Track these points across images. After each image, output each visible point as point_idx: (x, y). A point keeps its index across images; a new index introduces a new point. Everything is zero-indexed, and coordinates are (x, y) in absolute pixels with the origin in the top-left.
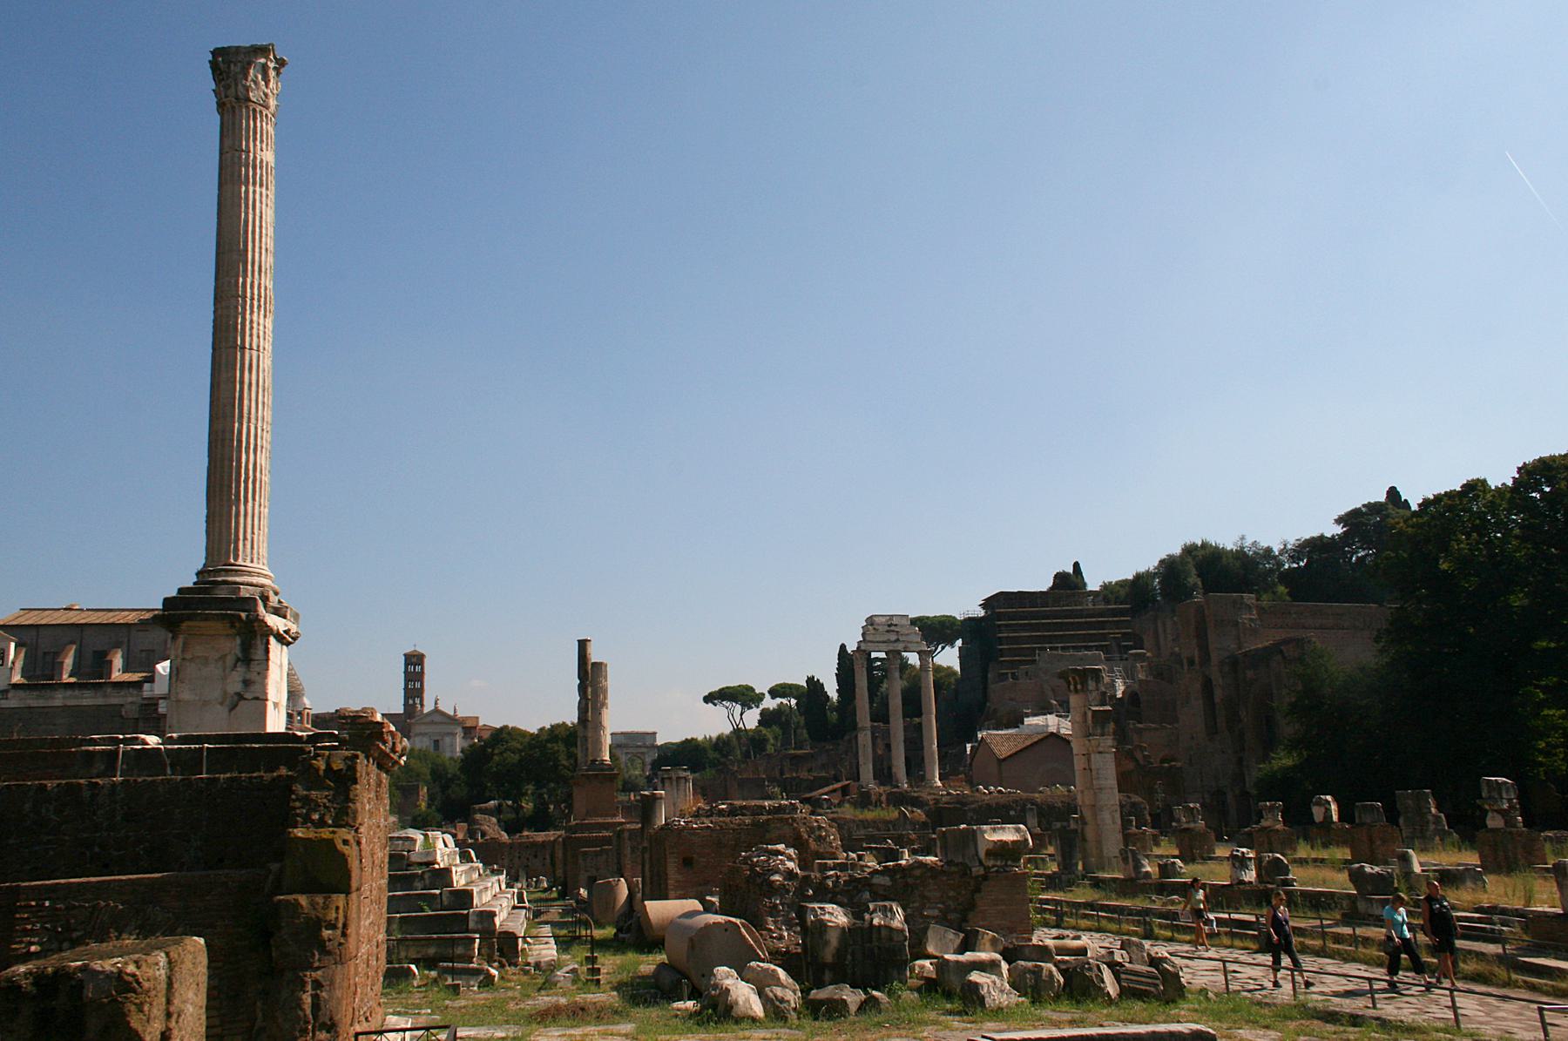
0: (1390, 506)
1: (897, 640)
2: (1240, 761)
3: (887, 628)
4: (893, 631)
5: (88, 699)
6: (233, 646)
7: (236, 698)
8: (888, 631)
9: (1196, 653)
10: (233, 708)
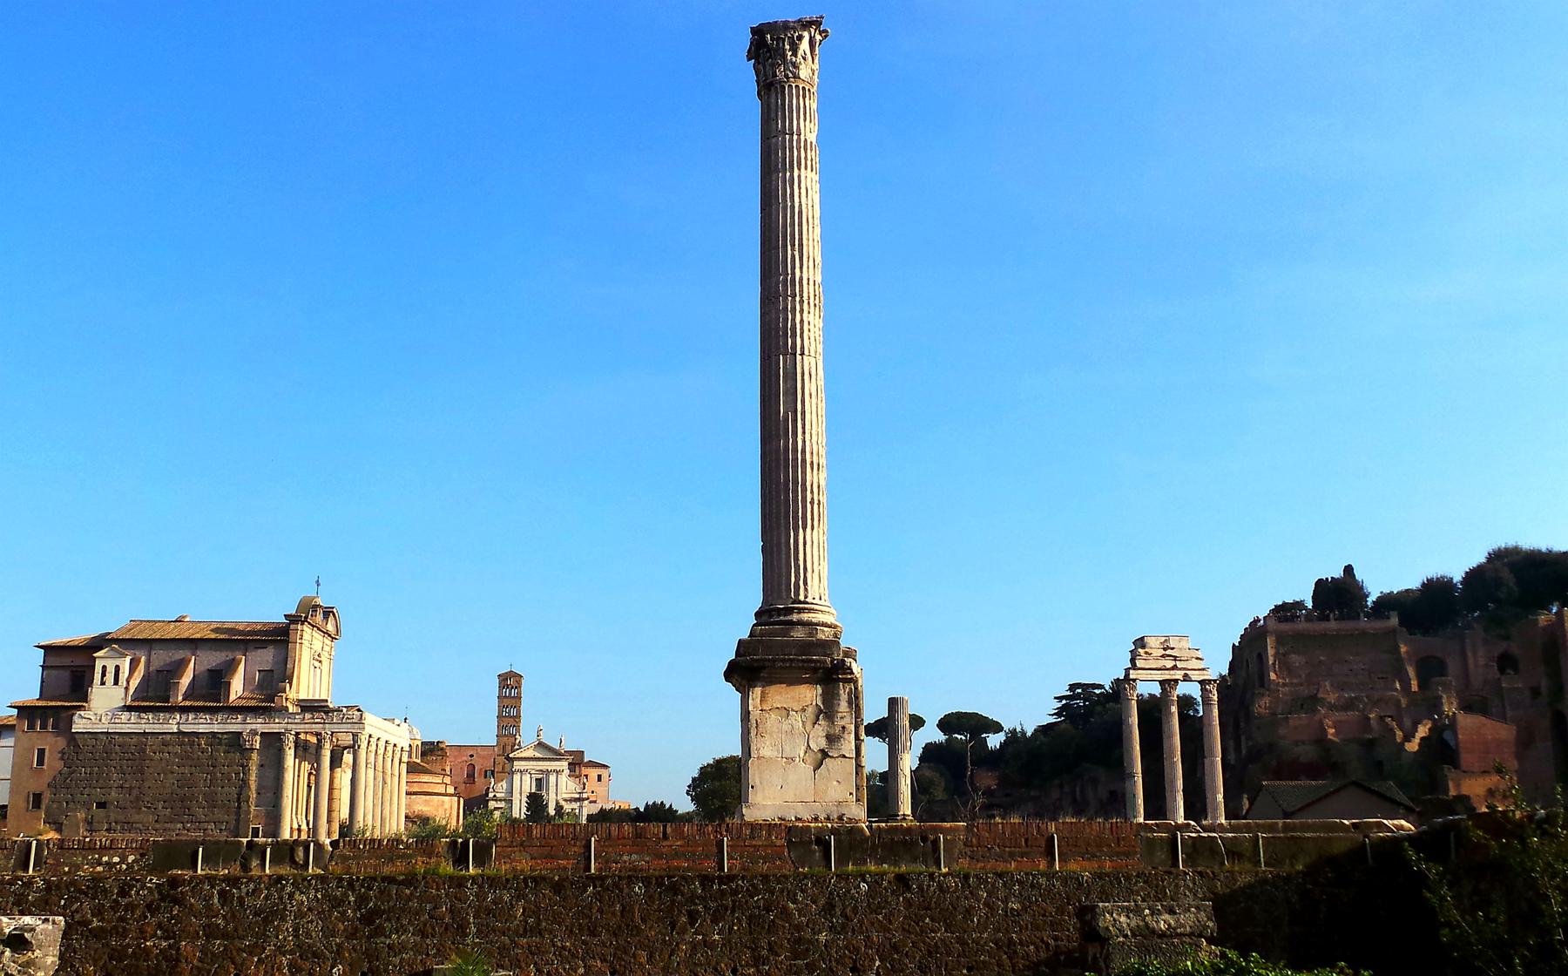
5: (203, 725)
7: (820, 755)
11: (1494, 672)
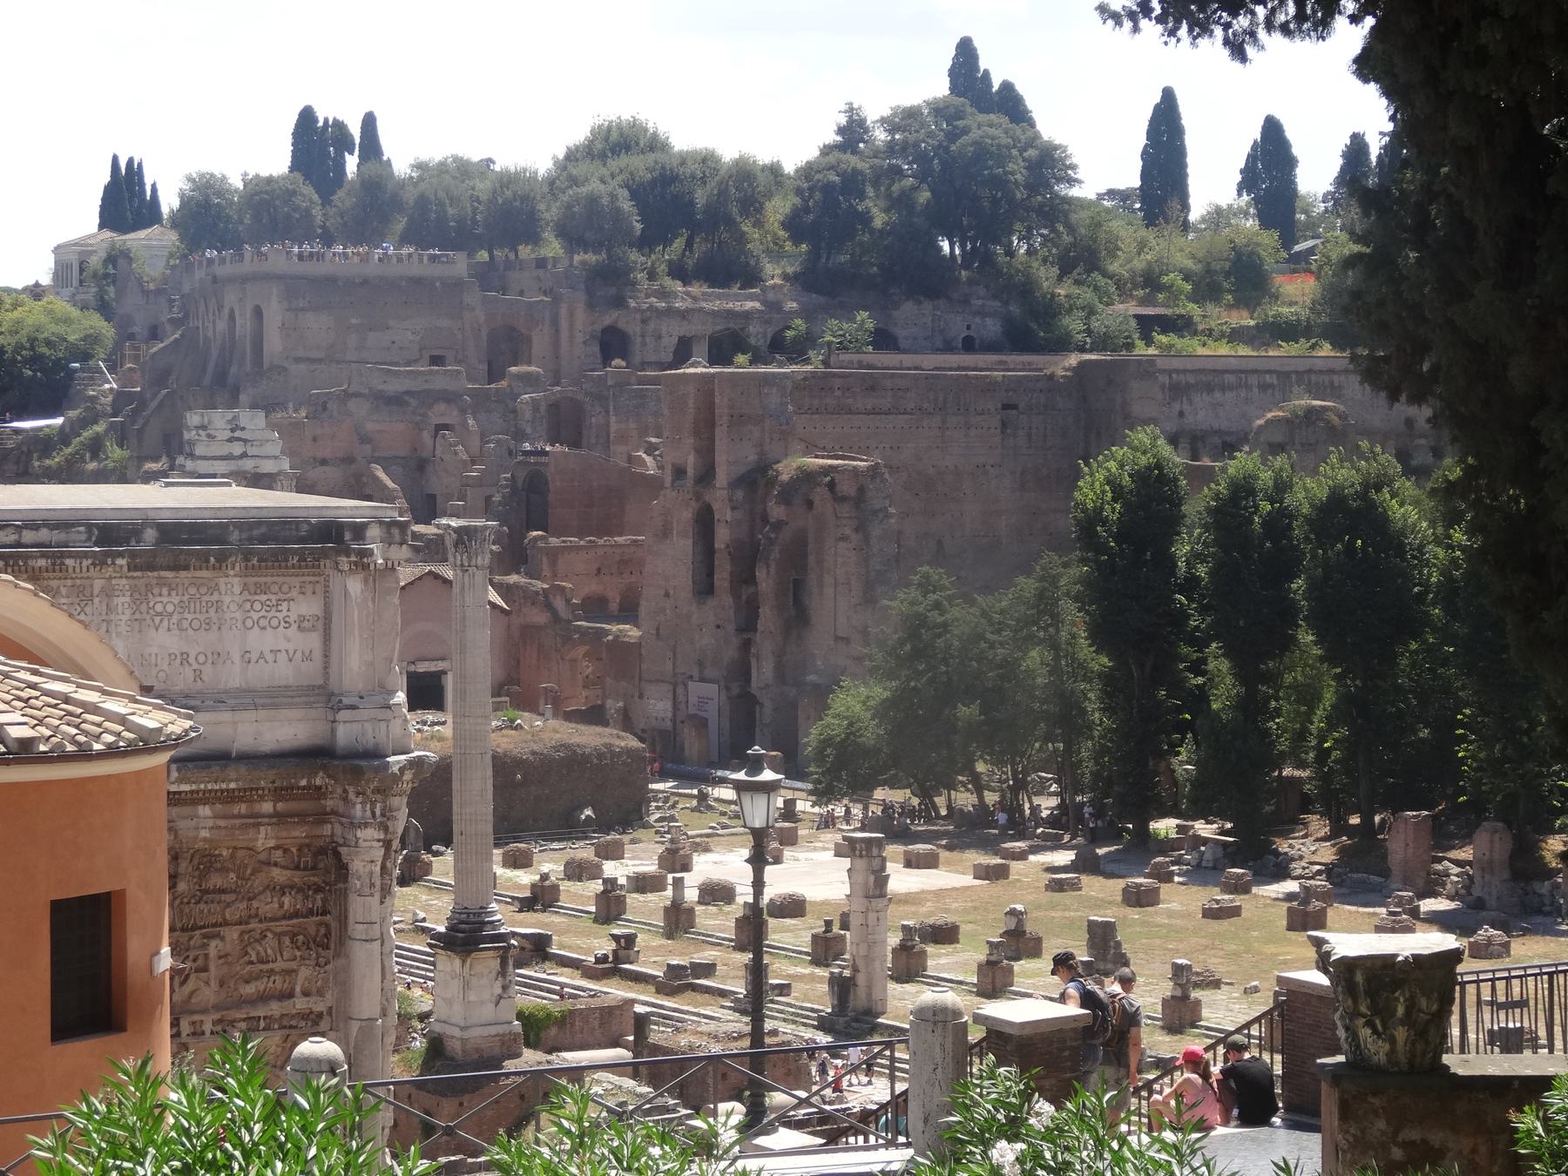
0: (969, 109)
1: (244, 455)
2: (746, 645)
3: (228, 434)
6: (495, 964)
8: (230, 440)
9: (691, 460)
10: (497, 1004)
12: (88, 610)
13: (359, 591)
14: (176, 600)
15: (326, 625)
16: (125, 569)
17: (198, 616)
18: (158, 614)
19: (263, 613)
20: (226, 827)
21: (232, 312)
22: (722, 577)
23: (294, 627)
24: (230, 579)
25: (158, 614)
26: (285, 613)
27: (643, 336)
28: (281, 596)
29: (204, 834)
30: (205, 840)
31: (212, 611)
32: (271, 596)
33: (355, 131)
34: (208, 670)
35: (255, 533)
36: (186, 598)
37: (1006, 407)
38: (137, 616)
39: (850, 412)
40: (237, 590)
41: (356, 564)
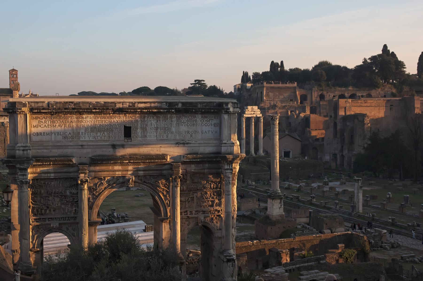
1: (254, 114)
2: (342, 147)
3: (251, 110)
4: (253, 111)
10: (280, 209)
11: (318, 99)
12: (167, 121)
13: (227, 118)
14: (186, 119)
15: (220, 125)
16: (175, 112)
17: (191, 123)
18: (182, 122)
19: (206, 122)
20: (198, 169)
21: (257, 93)
22: (338, 135)
23: (213, 126)
24: (199, 115)
25: (182, 122)
26: (211, 123)
27: (327, 96)
28: (210, 119)
29: (193, 171)
30: (193, 172)
31: (194, 122)
32: (208, 119)
33: (280, 64)
34: (194, 135)
35: (204, 105)
36: (188, 119)
37: (391, 106)
38: (178, 123)
39: (362, 106)
40: (200, 117)
41: (226, 111)
